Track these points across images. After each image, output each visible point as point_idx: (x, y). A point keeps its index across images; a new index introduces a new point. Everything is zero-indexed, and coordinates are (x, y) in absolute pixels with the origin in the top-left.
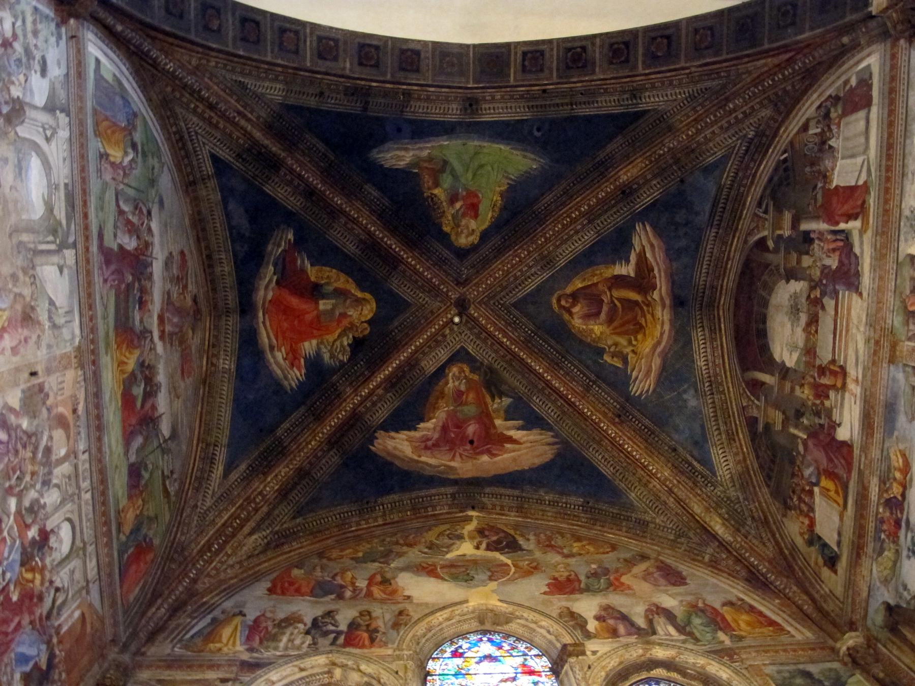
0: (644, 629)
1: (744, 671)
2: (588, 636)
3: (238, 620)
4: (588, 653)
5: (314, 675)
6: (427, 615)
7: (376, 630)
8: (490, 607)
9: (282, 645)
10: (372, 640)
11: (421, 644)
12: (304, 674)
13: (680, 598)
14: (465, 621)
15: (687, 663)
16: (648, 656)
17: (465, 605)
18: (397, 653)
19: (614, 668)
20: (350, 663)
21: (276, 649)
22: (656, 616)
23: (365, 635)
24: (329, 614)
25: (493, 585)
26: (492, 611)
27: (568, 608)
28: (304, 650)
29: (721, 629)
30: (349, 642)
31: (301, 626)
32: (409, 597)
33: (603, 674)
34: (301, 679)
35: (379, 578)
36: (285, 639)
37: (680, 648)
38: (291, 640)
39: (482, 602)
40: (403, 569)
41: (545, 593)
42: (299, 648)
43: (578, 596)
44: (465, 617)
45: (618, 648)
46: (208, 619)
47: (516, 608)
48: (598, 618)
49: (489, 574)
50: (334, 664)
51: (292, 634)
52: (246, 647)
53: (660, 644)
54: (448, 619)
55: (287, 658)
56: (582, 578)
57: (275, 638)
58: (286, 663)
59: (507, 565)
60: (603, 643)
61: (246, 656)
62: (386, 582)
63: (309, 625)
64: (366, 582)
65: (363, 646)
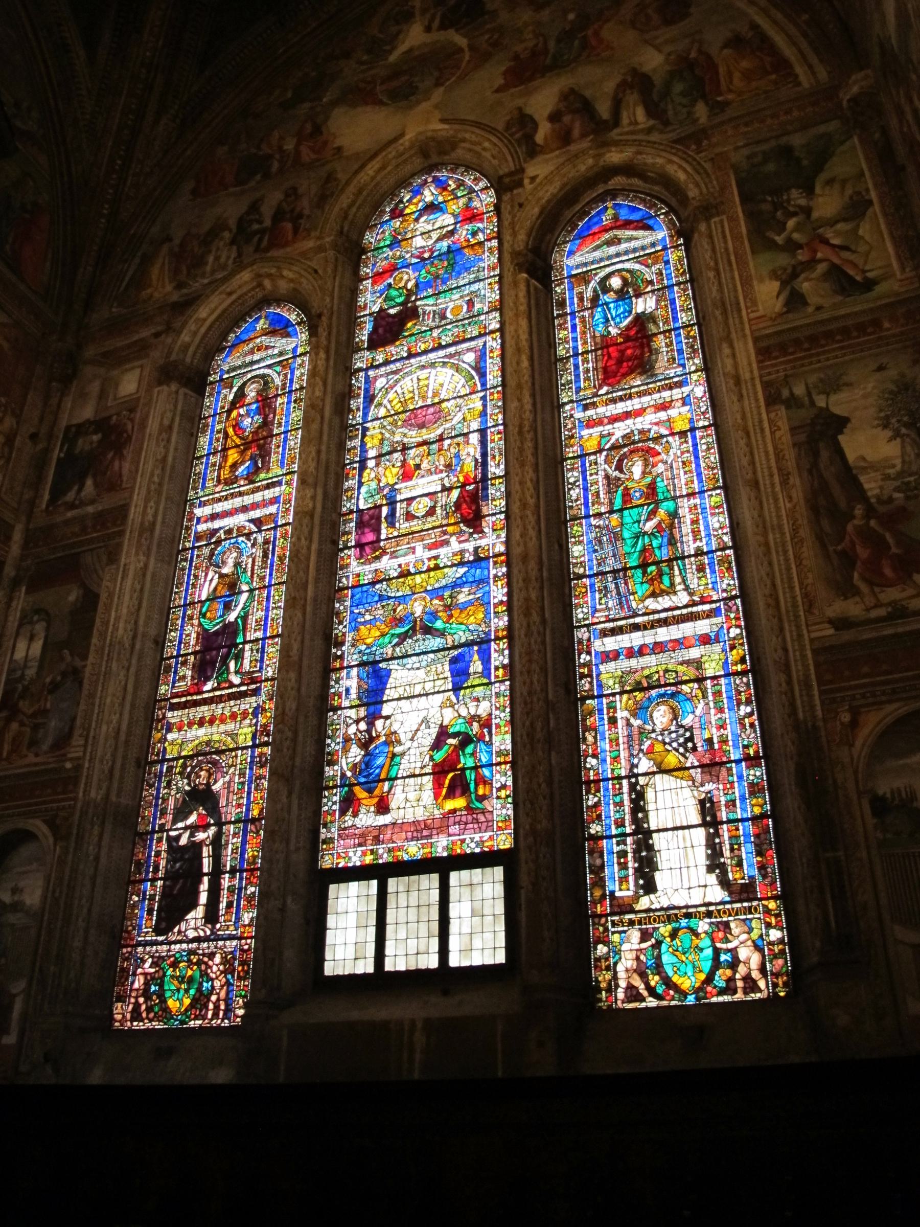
0: (606, 121)
1: (708, 166)
2: (533, 151)
3: (165, 249)
4: (526, 181)
5: (246, 294)
6: (357, 172)
7: (300, 216)
8: (429, 134)
9: (208, 268)
10: (296, 231)
11: (350, 217)
12: (234, 297)
13: (668, 48)
14: (405, 161)
15: (645, 164)
16: (601, 163)
17: (401, 141)
18: (318, 243)
19: (554, 195)
20: (273, 271)
21: (203, 276)
22: (628, 92)
23: (289, 226)
24: (254, 207)
25: (438, 95)
26: (433, 139)
27: (520, 109)
28: (229, 269)
29: (704, 97)
30: (272, 245)
31: (226, 235)
32: (339, 149)
33: (536, 210)
34: (233, 303)
35: (309, 127)
36: (211, 259)
37: (639, 143)
38: (217, 258)
39: (421, 129)
40: (335, 103)
41: (497, 91)
42: (224, 267)
43: (536, 83)
44: (404, 157)
45: (563, 164)
46: (137, 260)
47: (457, 127)
48: (554, 117)
49: (436, 74)
50: (259, 276)
51: (218, 249)
52: (174, 284)
53: (616, 143)
54: (383, 168)
55: (214, 285)
56: (552, 44)
57: (200, 262)
58: (213, 292)
59: (460, 50)
60: (547, 161)
61: (175, 297)
62: (317, 130)
63: (234, 231)
64: (295, 140)
65: (286, 244)
